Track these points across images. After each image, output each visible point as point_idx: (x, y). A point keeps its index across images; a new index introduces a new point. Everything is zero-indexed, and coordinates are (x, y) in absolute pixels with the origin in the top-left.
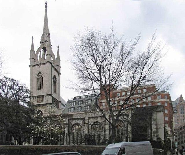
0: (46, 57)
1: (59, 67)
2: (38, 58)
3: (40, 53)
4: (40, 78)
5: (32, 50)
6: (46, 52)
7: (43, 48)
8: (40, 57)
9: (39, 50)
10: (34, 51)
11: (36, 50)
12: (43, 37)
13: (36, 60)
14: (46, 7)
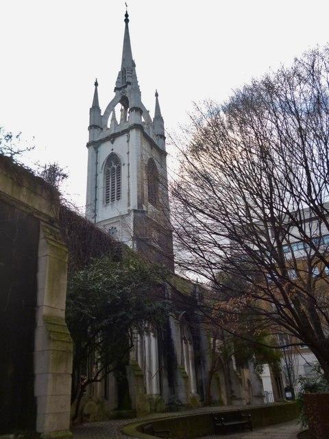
1: (161, 140)
4: (114, 169)
5: (95, 108)
7: (120, 102)
9: (111, 107)
10: (100, 111)
11: (103, 106)
13: (104, 130)
14: (127, 21)
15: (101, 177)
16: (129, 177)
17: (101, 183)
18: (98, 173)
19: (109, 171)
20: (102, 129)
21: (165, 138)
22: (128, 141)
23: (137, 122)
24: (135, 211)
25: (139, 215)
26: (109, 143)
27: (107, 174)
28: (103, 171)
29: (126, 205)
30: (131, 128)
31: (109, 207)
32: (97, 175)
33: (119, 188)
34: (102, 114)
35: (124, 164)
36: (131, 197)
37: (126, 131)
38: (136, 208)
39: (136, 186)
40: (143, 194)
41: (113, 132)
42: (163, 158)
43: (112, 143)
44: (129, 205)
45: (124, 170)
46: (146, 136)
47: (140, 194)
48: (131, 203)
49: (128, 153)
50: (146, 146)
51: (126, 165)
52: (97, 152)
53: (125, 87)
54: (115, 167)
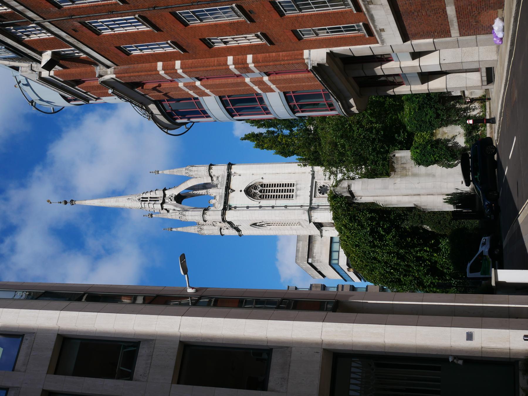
4: (261, 191)
15: (264, 202)
17: (272, 202)
26: (231, 195)
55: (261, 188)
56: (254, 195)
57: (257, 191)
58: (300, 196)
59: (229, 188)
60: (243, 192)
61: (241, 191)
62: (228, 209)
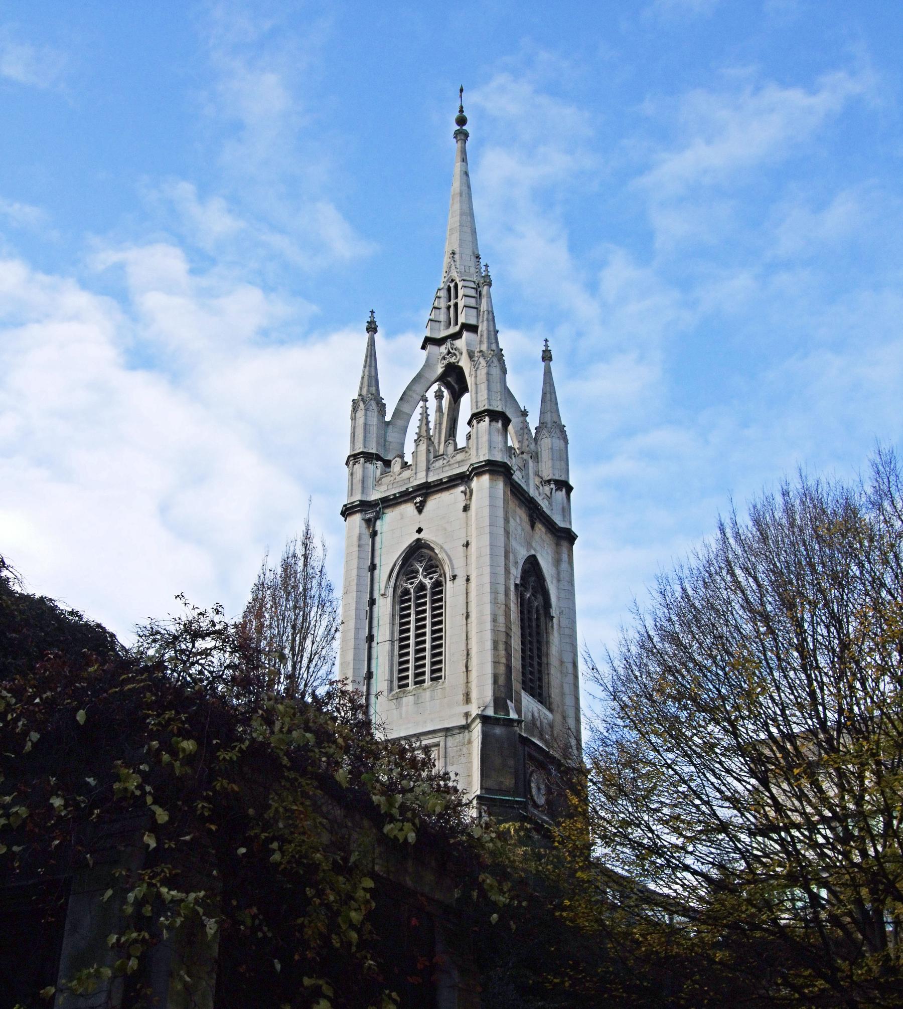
0: (462, 428)
1: (561, 494)
2: (409, 447)
3: (419, 410)
4: (422, 587)
6: (466, 400)
7: (442, 379)
8: (424, 436)
10: (382, 407)
12: (443, 304)
13: (396, 466)
15: (384, 608)
16: (467, 617)
17: (384, 631)
18: (376, 595)
19: (406, 592)
20: (387, 464)
21: (569, 489)
22: (466, 509)
23: (498, 457)
24: (485, 719)
25: (498, 731)
26: (409, 509)
27: (401, 598)
28: (390, 592)
29: (461, 697)
30: (477, 471)
31: (408, 700)
32: (372, 602)
33: (437, 647)
34: (388, 418)
35: (454, 577)
36: (474, 675)
37: (463, 479)
38: (490, 712)
39: (489, 645)
40: (509, 667)
41: (421, 479)
42: (564, 550)
43: (420, 510)
44: (467, 699)
45: (452, 592)
46: (517, 492)
47: (502, 669)
48: (474, 695)
49: (467, 545)
50: (520, 516)
51: (461, 580)
52: (374, 534)
53: (457, 336)
54: (428, 582)
55: (429, 586)
56: (413, 572)
57: (421, 577)
58: (398, 706)
59: (426, 496)
60: (417, 536)
61: (420, 531)
62: (368, 516)
